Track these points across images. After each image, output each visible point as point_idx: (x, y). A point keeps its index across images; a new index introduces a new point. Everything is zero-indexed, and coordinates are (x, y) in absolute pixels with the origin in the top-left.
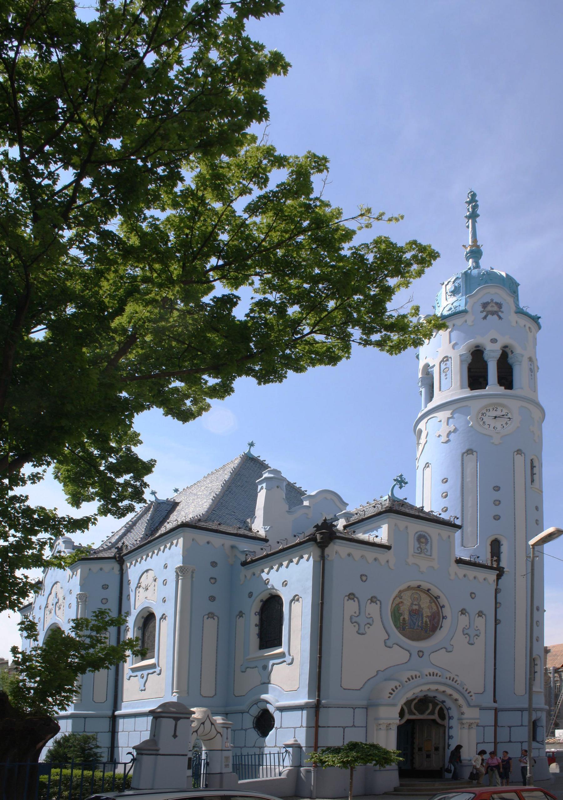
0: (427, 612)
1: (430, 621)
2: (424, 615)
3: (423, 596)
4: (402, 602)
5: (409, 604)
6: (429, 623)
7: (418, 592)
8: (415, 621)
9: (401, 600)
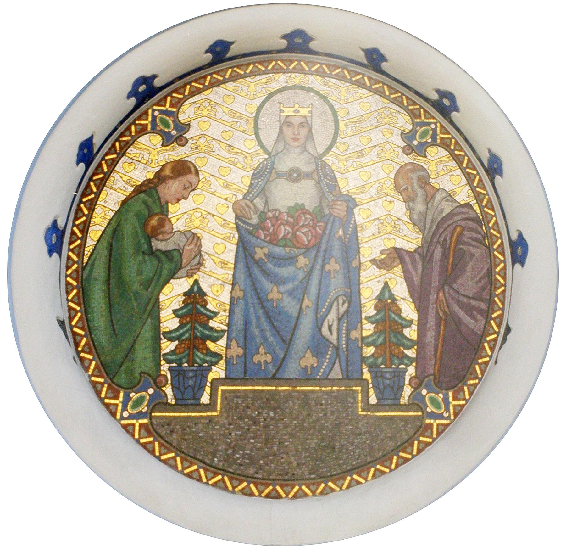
0: (384, 225)
1: (420, 297)
2: (370, 249)
3: (358, 103)
4: (182, 168)
5: (241, 179)
6: (409, 311)
7: (315, 82)
8: (290, 306)
9: (177, 153)
